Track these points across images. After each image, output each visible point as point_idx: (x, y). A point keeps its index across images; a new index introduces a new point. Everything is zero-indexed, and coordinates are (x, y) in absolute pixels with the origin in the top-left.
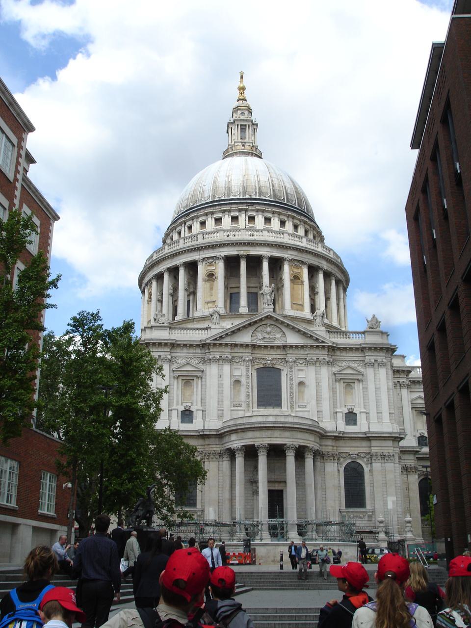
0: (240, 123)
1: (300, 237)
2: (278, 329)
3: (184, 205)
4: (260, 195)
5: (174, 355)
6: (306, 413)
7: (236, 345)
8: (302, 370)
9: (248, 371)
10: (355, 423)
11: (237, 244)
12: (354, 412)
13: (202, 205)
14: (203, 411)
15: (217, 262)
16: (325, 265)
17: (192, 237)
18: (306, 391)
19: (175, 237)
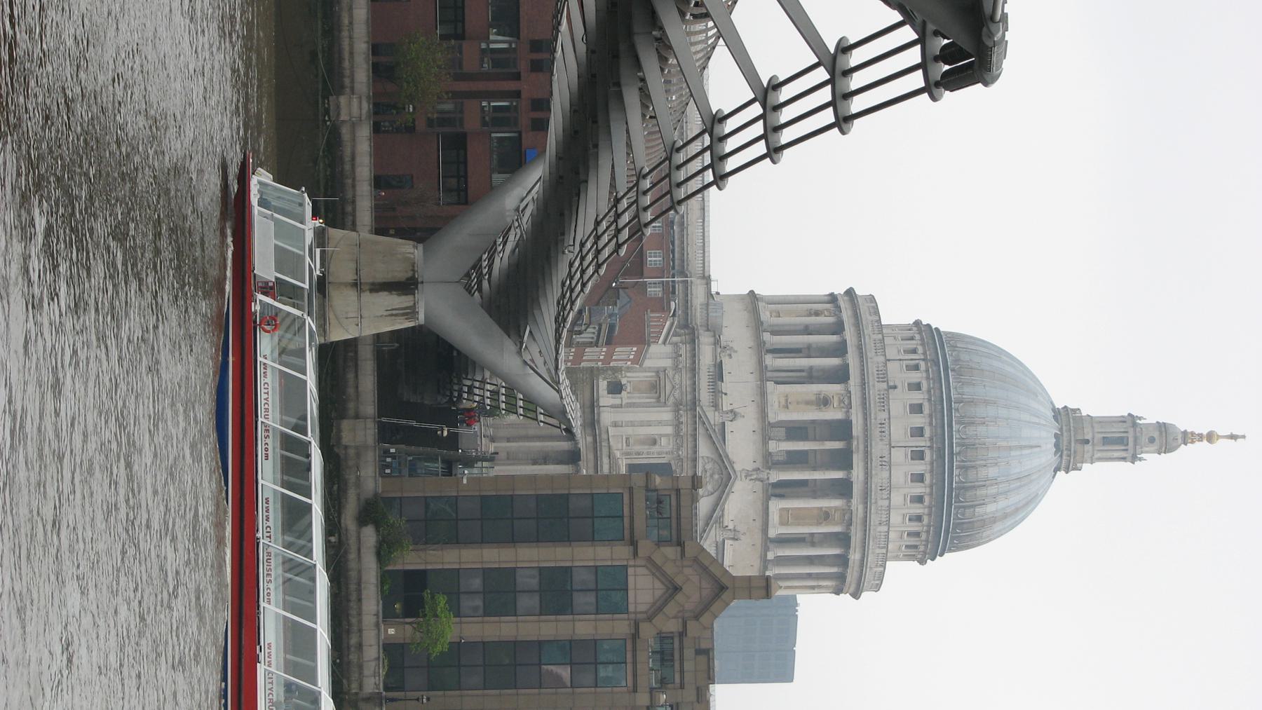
0: (1131, 436)
1: (888, 523)
2: (717, 487)
3: (964, 357)
5: (684, 372)
7: (695, 440)
9: (667, 453)
11: (867, 436)
15: (843, 410)
16: (854, 556)
19: (911, 345)
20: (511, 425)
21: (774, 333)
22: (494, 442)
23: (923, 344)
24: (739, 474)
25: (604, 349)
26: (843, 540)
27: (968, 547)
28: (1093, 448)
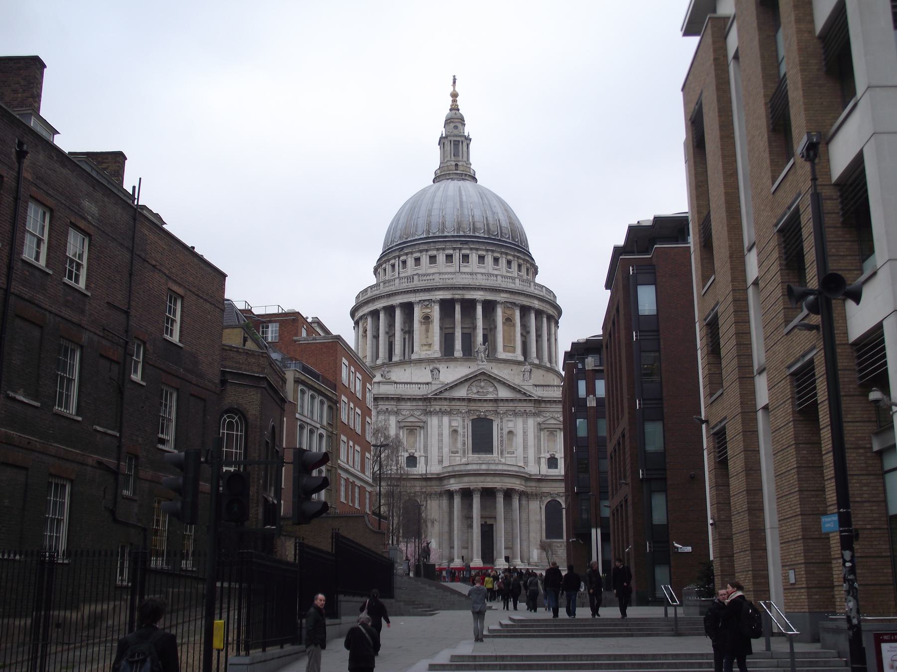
0: (453, 139)
1: (513, 279)
3: (398, 234)
4: (474, 231)
5: (400, 407)
6: (514, 459)
7: (454, 399)
8: (511, 421)
9: (464, 422)
10: (556, 467)
12: (556, 457)
13: (416, 239)
14: (425, 457)
16: (536, 304)
17: (407, 277)
18: (514, 438)
20: (440, 545)
21: (377, 357)
22: (453, 560)
23: (389, 260)
24: (481, 367)
25: (344, 398)
26: (525, 310)
27: (527, 240)
28: (461, 161)
